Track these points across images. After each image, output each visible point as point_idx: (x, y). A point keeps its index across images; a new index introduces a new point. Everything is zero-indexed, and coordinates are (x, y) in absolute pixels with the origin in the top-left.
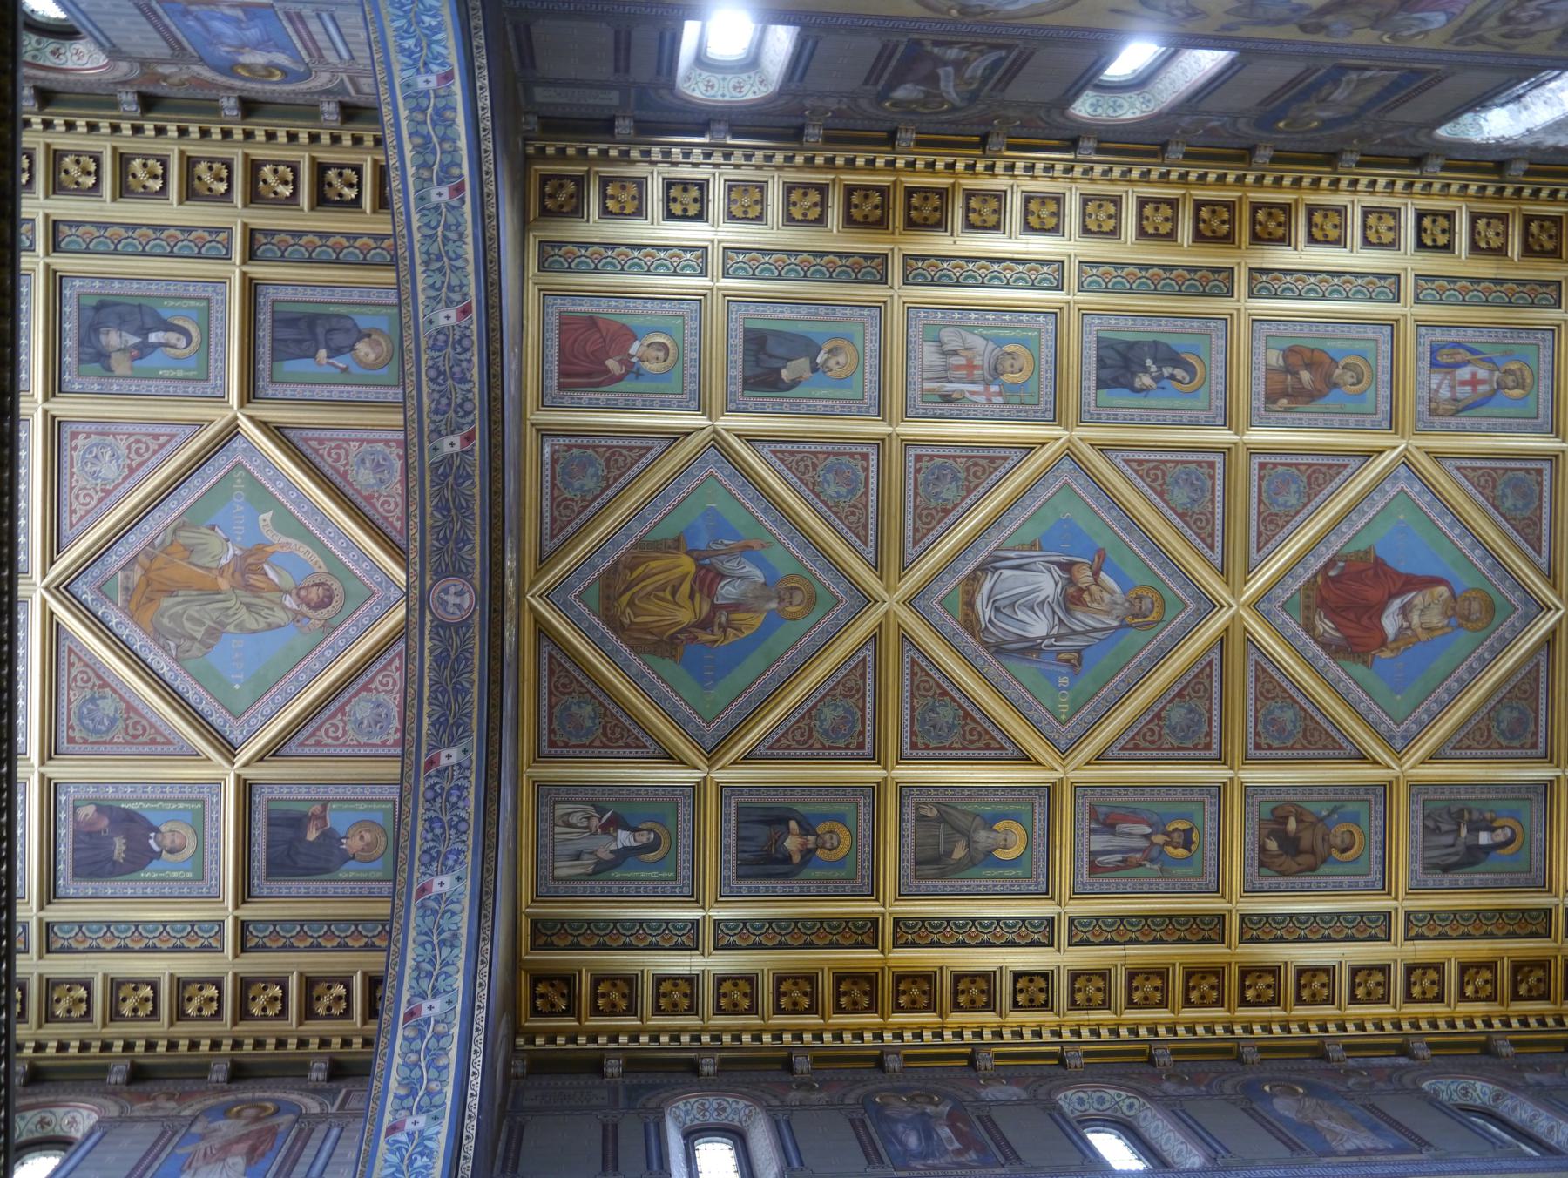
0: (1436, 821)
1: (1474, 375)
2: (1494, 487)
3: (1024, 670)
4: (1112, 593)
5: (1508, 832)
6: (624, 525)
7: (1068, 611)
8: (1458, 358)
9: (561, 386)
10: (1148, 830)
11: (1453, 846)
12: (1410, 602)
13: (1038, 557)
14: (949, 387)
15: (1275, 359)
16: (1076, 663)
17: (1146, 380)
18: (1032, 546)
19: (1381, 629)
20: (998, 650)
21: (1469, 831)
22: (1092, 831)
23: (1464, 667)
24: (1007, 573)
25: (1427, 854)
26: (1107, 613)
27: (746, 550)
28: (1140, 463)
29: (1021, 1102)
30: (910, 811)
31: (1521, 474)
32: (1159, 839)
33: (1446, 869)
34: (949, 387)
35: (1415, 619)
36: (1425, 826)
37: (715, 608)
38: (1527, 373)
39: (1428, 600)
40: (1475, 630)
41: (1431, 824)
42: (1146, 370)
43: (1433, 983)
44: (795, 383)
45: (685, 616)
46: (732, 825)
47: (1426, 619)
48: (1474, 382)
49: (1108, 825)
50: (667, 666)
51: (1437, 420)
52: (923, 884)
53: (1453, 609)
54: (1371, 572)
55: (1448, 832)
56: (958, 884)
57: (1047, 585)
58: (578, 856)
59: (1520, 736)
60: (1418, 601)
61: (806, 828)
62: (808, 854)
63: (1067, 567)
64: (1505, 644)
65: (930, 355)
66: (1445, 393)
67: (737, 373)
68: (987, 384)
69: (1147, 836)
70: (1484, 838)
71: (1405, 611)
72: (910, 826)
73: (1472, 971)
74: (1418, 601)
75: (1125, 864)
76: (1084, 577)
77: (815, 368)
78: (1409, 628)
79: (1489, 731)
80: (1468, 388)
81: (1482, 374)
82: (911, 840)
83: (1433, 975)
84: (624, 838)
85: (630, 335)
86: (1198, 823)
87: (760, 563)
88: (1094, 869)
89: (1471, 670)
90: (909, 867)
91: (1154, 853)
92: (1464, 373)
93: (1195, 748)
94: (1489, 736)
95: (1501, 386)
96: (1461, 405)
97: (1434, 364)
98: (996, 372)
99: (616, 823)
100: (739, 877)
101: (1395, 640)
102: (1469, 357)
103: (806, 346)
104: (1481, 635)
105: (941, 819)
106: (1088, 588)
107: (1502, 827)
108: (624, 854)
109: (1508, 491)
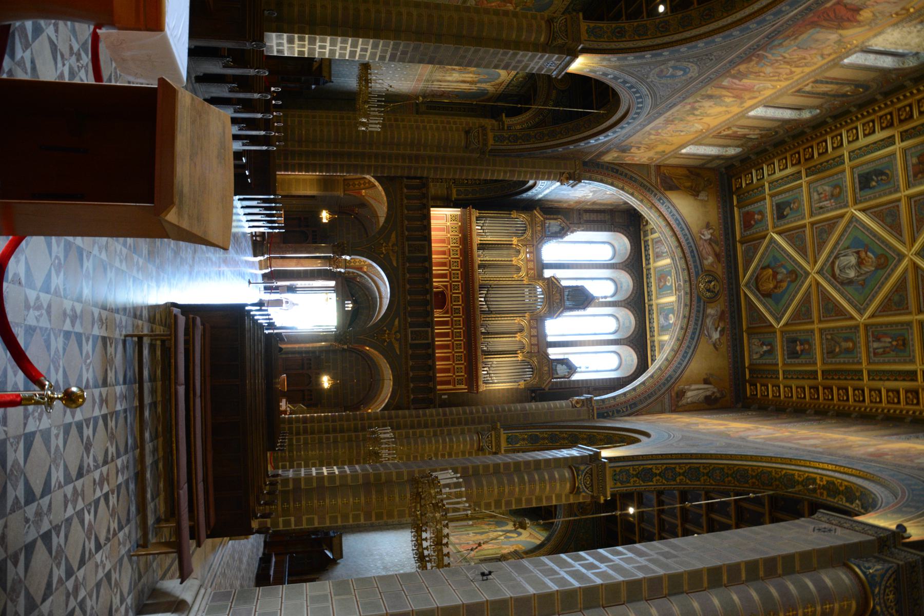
3: (850, 289)
4: (871, 258)
6: (758, 265)
7: (860, 267)
9: (745, 231)
10: (890, 340)
13: (849, 251)
14: (821, 204)
15: (915, 160)
16: (864, 284)
17: (874, 183)
18: (848, 248)
20: (842, 283)
22: (873, 341)
24: (842, 258)
26: (871, 265)
27: (783, 266)
28: (875, 212)
30: (824, 337)
32: (894, 343)
34: (821, 204)
37: (777, 282)
42: (873, 180)
44: (787, 215)
45: (771, 286)
46: (785, 344)
49: (878, 339)
50: (770, 300)
52: (829, 360)
56: (838, 360)
57: (853, 260)
58: (757, 353)
61: (801, 344)
62: (802, 351)
63: (858, 253)
65: (816, 196)
67: (775, 216)
68: (830, 200)
69: (890, 342)
72: (824, 341)
75: (884, 353)
76: (863, 255)
77: (791, 209)
82: (825, 346)
84: (765, 348)
85: (754, 214)
86: (906, 336)
87: (785, 268)
88: (875, 354)
90: (825, 356)
91: (893, 348)
93: (903, 309)
98: (832, 195)
99: (763, 344)
100: (788, 358)
103: (787, 204)
105: (832, 339)
106: (864, 259)
108: (765, 352)
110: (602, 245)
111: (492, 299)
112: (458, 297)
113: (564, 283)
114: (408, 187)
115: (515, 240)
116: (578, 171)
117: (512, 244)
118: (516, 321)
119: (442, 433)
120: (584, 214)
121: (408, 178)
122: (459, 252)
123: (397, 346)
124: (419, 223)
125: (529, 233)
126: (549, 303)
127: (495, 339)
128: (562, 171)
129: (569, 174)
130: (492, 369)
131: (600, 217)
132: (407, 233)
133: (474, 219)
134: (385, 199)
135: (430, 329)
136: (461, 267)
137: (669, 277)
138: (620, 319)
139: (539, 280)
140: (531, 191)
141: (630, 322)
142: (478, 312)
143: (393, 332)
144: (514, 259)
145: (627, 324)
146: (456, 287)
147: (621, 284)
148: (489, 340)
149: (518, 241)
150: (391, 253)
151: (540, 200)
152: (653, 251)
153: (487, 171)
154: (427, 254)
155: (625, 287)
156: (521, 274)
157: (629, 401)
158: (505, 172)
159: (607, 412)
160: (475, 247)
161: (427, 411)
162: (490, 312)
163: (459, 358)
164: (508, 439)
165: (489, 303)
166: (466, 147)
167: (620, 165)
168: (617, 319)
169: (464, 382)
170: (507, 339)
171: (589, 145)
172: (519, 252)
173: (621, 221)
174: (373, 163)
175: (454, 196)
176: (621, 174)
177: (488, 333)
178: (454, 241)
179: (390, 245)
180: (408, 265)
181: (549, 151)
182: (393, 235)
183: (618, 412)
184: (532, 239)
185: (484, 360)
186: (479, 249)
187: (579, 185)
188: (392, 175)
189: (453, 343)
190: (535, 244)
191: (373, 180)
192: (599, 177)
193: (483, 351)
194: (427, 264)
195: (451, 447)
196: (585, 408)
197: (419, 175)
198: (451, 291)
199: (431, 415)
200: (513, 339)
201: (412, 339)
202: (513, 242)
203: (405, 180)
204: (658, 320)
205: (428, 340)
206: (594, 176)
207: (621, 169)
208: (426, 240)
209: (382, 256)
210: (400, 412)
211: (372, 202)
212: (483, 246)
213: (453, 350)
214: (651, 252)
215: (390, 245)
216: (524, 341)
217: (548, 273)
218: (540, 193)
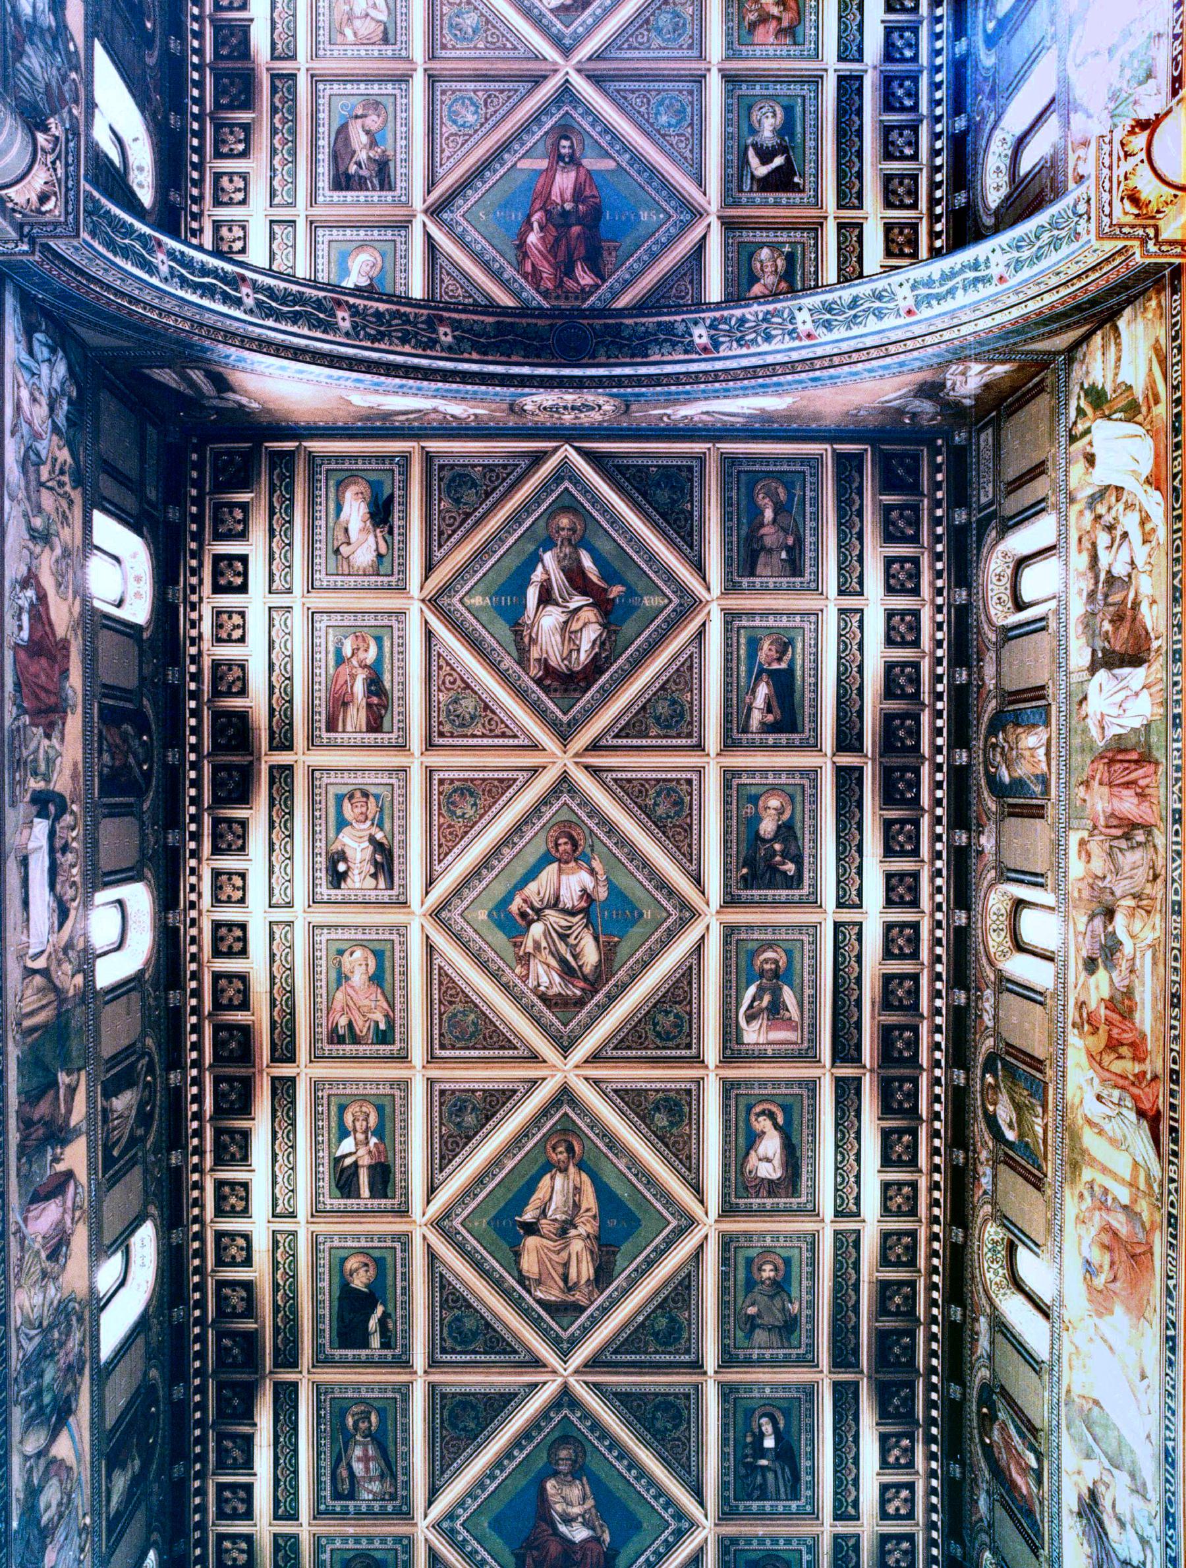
0: (754, 1489)
1: (359, 1460)
2: (458, 1439)
5: (764, 1420)
8: (345, 1474)
11: (775, 1472)
12: (560, 1516)
19: (585, 1541)
21: (762, 1457)
23: (617, 1464)
25: (783, 1496)
29: (995, 1552)
31: (446, 1413)
33: (796, 1478)
35: (576, 1510)
36: (758, 1499)
38: (355, 1409)
39: (558, 1498)
40: (585, 1454)
41: (757, 1493)
43: (901, 135)
47: (575, 1500)
48: (365, 1459)
51: (401, 1493)
53: (566, 1475)
54: (535, 1553)
55: (764, 1477)
59: (678, 1411)
60: (559, 1508)
64: (597, 1425)
66: (375, 1487)
70: (769, 1443)
71: (568, 1520)
73: (892, 198)
74: (559, 1508)
78: (583, 1516)
79: (674, 1439)
80: (371, 1465)
81: (358, 1452)
83: (894, 135)
89: (620, 1458)
92: (358, 1468)
94: (679, 1439)
95: (368, 1434)
96: (386, 1471)
97: (352, 1496)
101: (593, 1529)
102: (344, 1463)
104: (589, 1448)
107: (760, 1426)
109: (461, 1425)
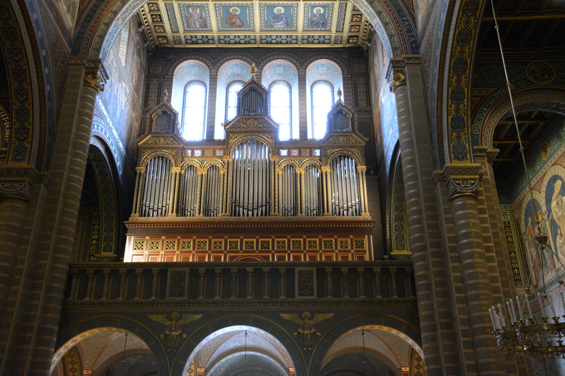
110: (188, 95)
111: (251, 201)
112: (247, 243)
113: (233, 114)
114: (82, 295)
115: (175, 170)
116: (85, 62)
117: (180, 174)
118: (280, 173)
119: (453, 250)
120: (149, 106)
121: (67, 294)
122: (186, 240)
123: (320, 317)
124: (139, 279)
125: (167, 153)
126: (259, 132)
127: (303, 199)
128: (82, 82)
129: (87, 74)
130: (341, 204)
131: (154, 89)
132: (153, 298)
133: (143, 219)
134: (96, 331)
135: (297, 269)
136: (207, 238)
137: (231, 10)
138: (275, 79)
139: (228, 144)
140: (113, 152)
141: (279, 66)
142: (268, 218)
143: (300, 322)
144: (199, 173)
145: (280, 70)
146: (234, 245)
147: (233, 75)
148: (304, 206)
149: (176, 166)
150: (181, 322)
151: (127, 149)
152: (198, 31)
153: (70, 179)
154: (187, 270)
155: (237, 70)
156: (219, 165)
157: (395, 18)
158: (76, 155)
159: (411, 44)
160: (181, 219)
161: (418, 273)
162: (268, 203)
163: (328, 244)
164: (458, 159)
165: (255, 205)
166: (27, 202)
167: (81, 12)
168: (274, 82)
169: (359, 239)
170: (303, 184)
171: (41, 22)
172: (191, 167)
173: (160, 68)
174: (31, 347)
175: (111, 254)
176: (94, 12)
177: (295, 208)
178: (170, 245)
179: (168, 323)
180: (201, 297)
181: (48, 88)
182: (154, 318)
183: (409, 31)
184: (175, 148)
185: (330, 212)
186: (184, 215)
187: (104, 64)
188: (58, 317)
189: (308, 252)
190: (181, 146)
191: (63, 351)
192: (96, 39)
193: (318, 214)
194: (202, 270)
195: (477, 235)
196: (406, 69)
197: (64, 277)
198: (238, 252)
199: (426, 267)
200: (303, 177)
201: (311, 294)
202: (178, 172)
203: (70, 299)
204: (279, 31)
205: (312, 272)
206: (94, 44)
207: (87, 11)
208: (166, 271)
209: (185, 336)
210: (422, 313)
211: (104, 359)
212: (181, 210)
213: (317, 251)
214: (199, 35)
215: (168, 323)
216: (306, 165)
217: (220, 134)
218: (117, 144)
